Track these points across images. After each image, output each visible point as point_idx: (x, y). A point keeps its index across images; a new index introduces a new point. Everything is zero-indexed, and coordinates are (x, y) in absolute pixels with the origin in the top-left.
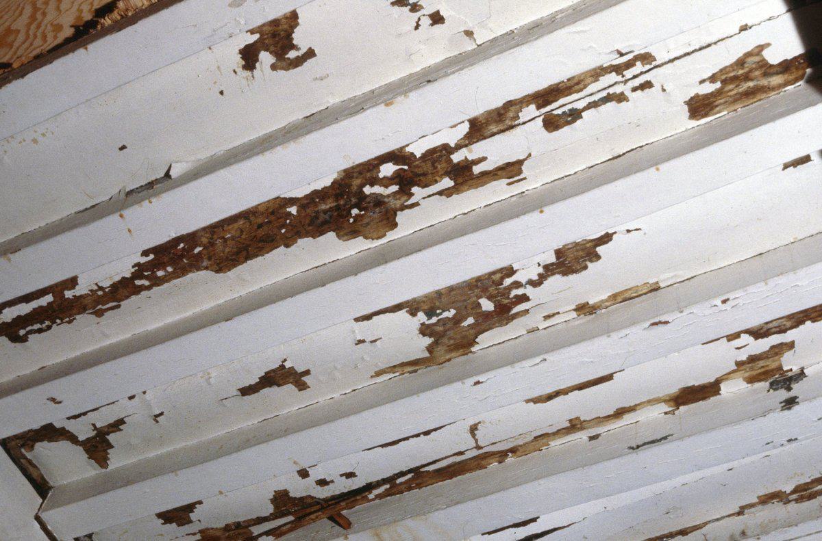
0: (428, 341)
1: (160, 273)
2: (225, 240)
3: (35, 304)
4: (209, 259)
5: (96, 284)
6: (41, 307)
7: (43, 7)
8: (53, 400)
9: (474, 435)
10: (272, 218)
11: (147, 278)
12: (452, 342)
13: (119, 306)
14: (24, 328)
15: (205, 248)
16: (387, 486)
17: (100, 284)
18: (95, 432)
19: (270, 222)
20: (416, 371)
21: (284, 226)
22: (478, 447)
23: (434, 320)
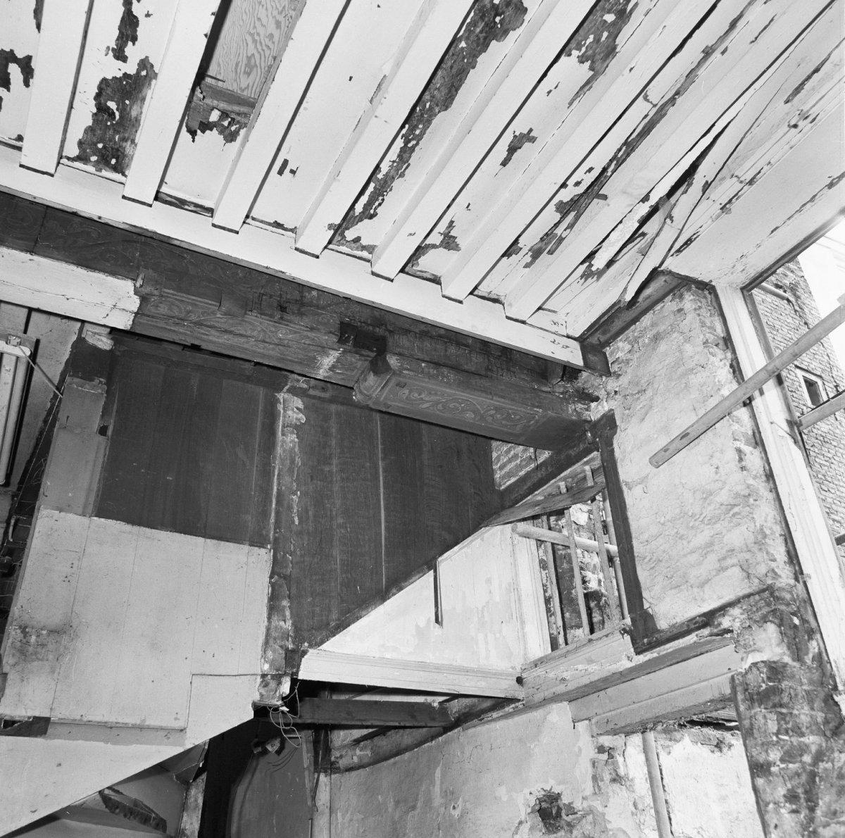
0: (588, 64)
1: (418, 132)
2: (439, 89)
4: (437, 105)
7: (255, 31)
8: (411, 234)
9: (648, 101)
10: (455, 57)
11: (413, 139)
12: (602, 55)
13: (409, 165)
15: (431, 101)
16: (615, 162)
19: (455, 61)
20: (591, 87)
21: (464, 58)
22: (655, 106)
23: (584, 49)
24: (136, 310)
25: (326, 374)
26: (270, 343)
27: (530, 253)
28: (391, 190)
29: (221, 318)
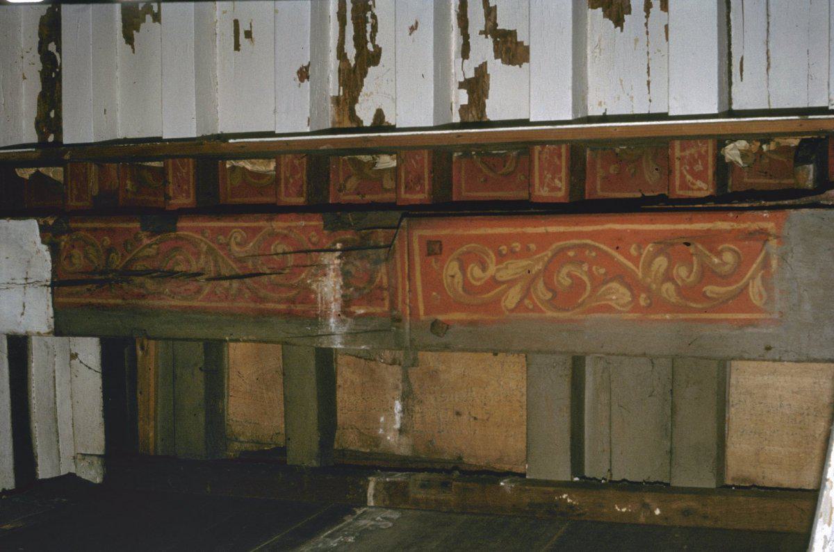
3: (349, 15)
6: (353, 10)
8: (413, 29)
14: (367, 42)
18: (489, 36)
24: (47, 275)
25: (345, 329)
26: (231, 278)
29: (150, 246)
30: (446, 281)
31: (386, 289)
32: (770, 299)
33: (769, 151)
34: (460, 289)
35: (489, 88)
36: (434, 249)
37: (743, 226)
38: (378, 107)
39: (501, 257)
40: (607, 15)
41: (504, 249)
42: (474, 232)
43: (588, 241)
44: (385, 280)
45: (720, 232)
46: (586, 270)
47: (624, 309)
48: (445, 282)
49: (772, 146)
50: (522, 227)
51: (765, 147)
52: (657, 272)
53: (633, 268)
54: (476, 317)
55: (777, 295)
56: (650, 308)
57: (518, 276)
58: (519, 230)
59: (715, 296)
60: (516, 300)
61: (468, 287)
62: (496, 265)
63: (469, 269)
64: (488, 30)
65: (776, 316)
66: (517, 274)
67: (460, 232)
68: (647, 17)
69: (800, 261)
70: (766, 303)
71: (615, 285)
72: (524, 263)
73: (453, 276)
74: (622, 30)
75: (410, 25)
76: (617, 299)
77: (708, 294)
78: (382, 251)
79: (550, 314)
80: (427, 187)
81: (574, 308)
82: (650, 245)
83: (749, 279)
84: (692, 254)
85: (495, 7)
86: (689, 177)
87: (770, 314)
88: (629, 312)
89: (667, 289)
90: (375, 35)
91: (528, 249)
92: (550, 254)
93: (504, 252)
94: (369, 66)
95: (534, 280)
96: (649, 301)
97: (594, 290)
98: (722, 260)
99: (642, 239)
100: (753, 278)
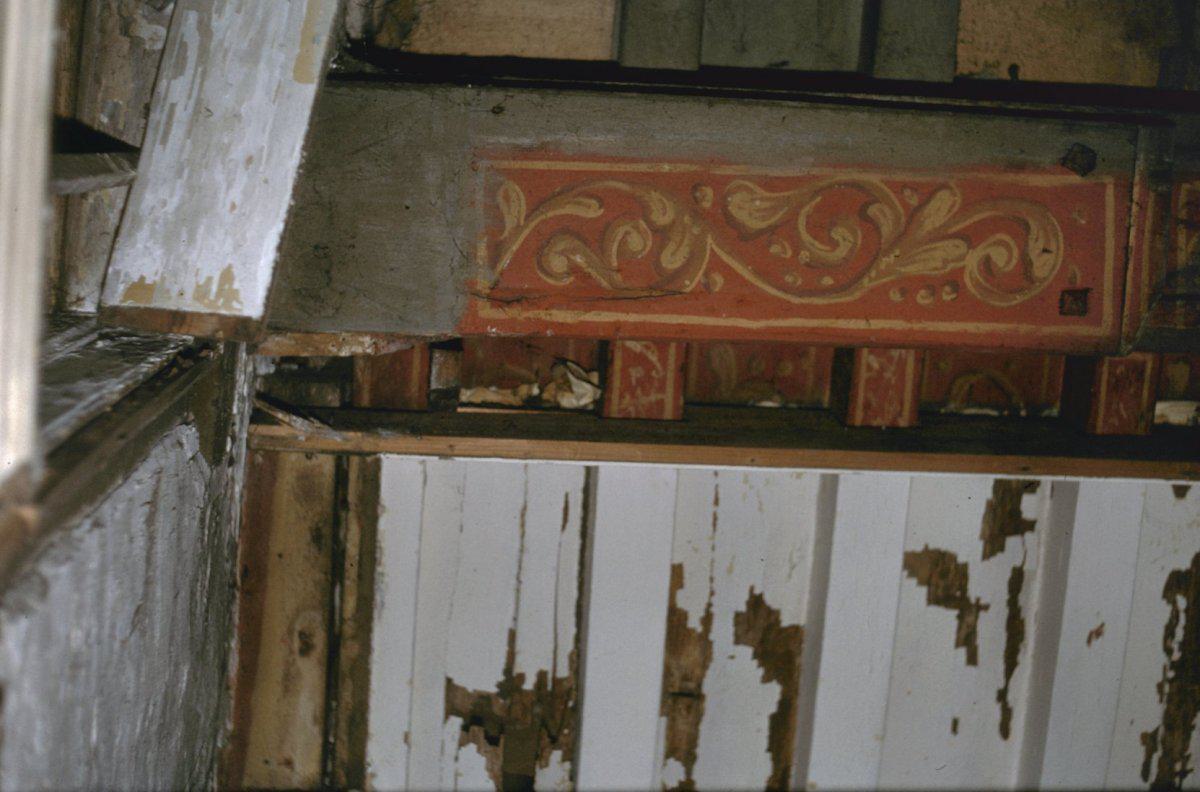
5: (1192, 770)
8: (1098, 633)
14: (1187, 611)
17: (1190, 776)
18: (973, 600)
27: (694, 623)
28: (1160, 687)
30: (1058, 244)
31: (1182, 221)
32: (491, 192)
33: (530, 383)
34: (1032, 223)
35: (985, 517)
36: (1076, 300)
37: (531, 314)
38: (1182, 502)
39: (954, 281)
40: (773, 615)
41: (947, 296)
42: (1001, 327)
43: (796, 300)
44: (1182, 239)
45: (569, 307)
46: (802, 252)
47: (741, 182)
48: (1062, 246)
49: (523, 390)
50: (911, 330)
51: (536, 391)
52: (680, 244)
53: (716, 249)
54: (1010, 177)
55: (480, 196)
56: (694, 184)
57: (925, 247)
58: (917, 326)
59: (582, 199)
60: (934, 204)
61: (1020, 229)
62: (962, 269)
63: (1014, 261)
64: (974, 610)
65: (483, 164)
66: (926, 251)
67: (1024, 328)
68: (710, 605)
69: (440, 252)
70: (501, 184)
71: (755, 224)
72: (912, 270)
73: (1045, 251)
74: (752, 589)
75: (1100, 639)
76: (753, 200)
77: (594, 202)
78: (1180, 291)
79: (873, 178)
80: (1105, 368)
81: (830, 187)
82: (688, 290)
83: (526, 226)
84: (619, 271)
85: (958, 645)
86: (653, 358)
87: (492, 166)
88: (735, 177)
89: (664, 214)
90: (1171, 621)
91: (903, 292)
92: (866, 281)
93: (947, 289)
94: (1188, 572)
95: (898, 239)
96: (698, 194)
97: (789, 222)
98: (568, 259)
99: (700, 297)
100: (518, 229)
